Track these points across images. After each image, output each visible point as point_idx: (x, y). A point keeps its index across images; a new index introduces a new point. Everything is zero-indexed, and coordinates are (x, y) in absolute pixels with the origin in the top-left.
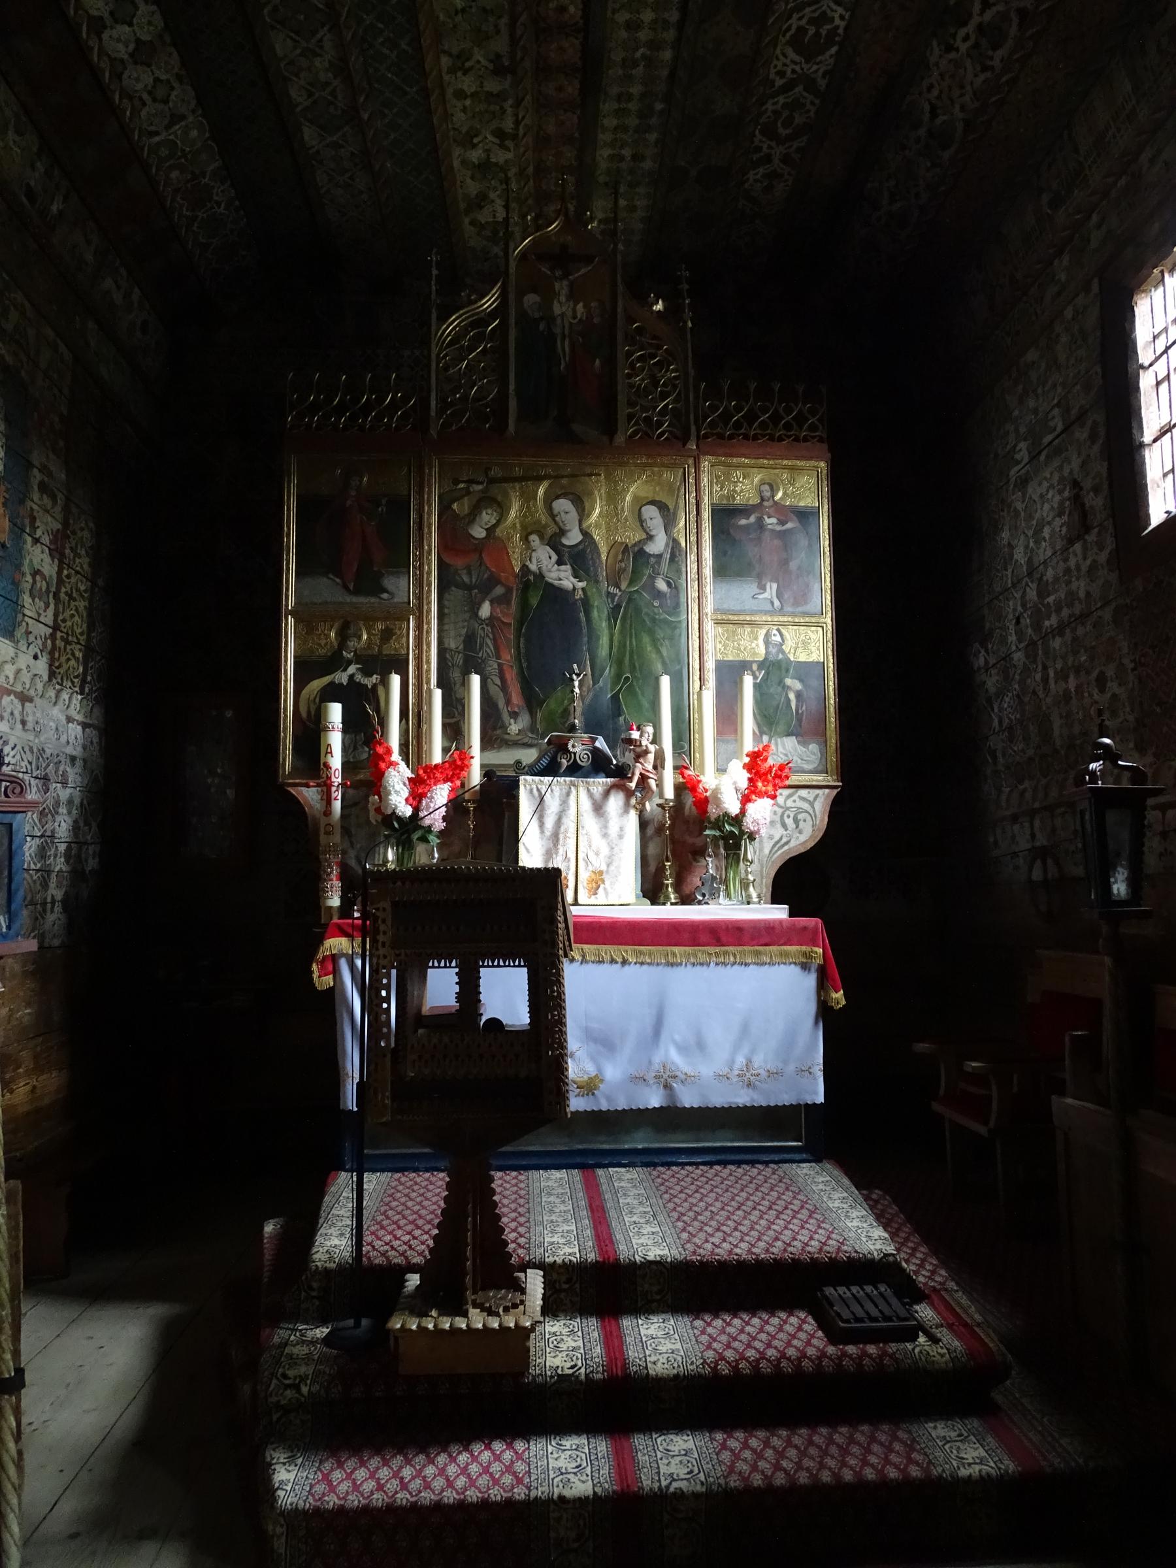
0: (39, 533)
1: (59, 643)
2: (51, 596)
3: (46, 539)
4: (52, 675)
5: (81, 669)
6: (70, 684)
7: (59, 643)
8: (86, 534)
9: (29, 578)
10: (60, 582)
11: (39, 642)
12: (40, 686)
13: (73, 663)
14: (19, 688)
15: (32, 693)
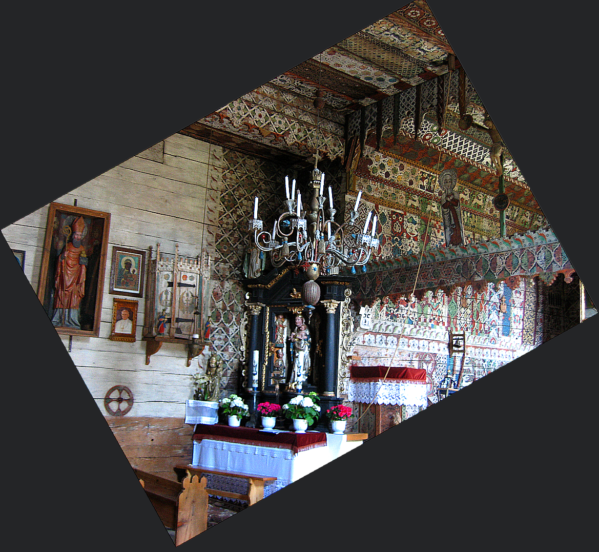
0: (516, 305)
1: (525, 333)
2: (521, 320)
3: (519, 305)
4: (523, 342)
5: (533, 338)
6: (529, 343)
7: (525, 333)
8: (533, 298)
9: (513, 318)
10: (524, 315)
11: (518, 335)
12: (518, 346)
13: (530, 337)
14: (511, 349)
15: (516, 349)
